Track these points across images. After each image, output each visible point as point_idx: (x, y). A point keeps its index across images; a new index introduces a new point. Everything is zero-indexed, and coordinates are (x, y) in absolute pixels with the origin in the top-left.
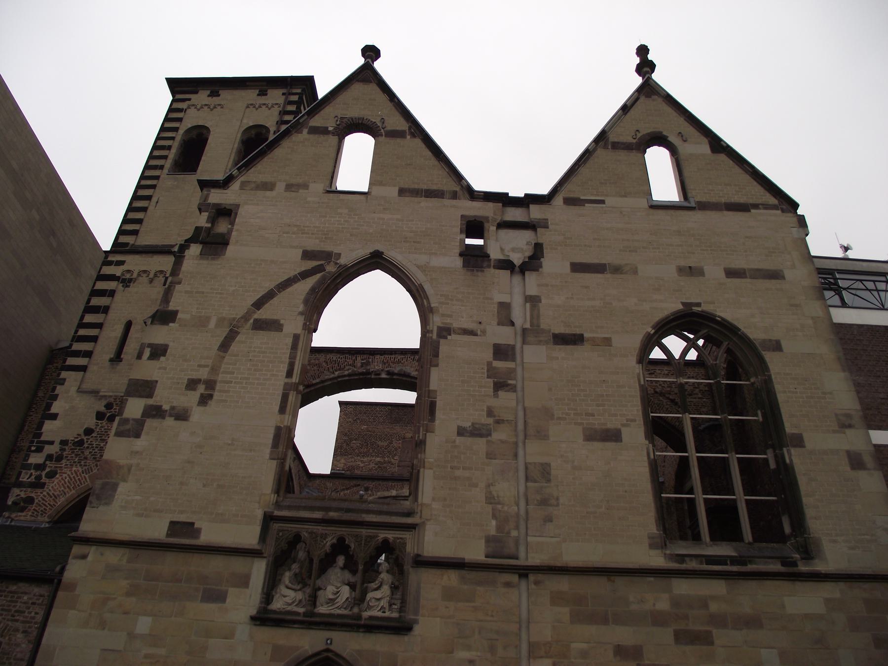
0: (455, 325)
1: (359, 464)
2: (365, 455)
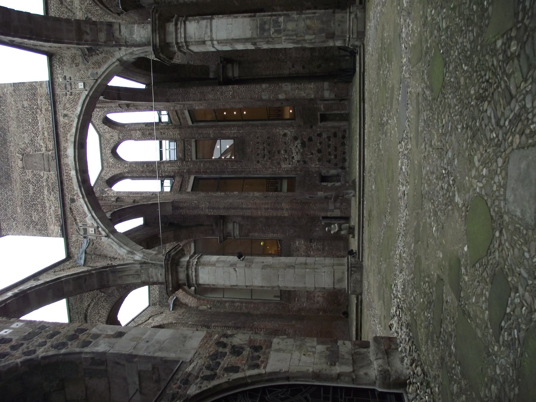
1: (53, 211)
2: (43, 206)
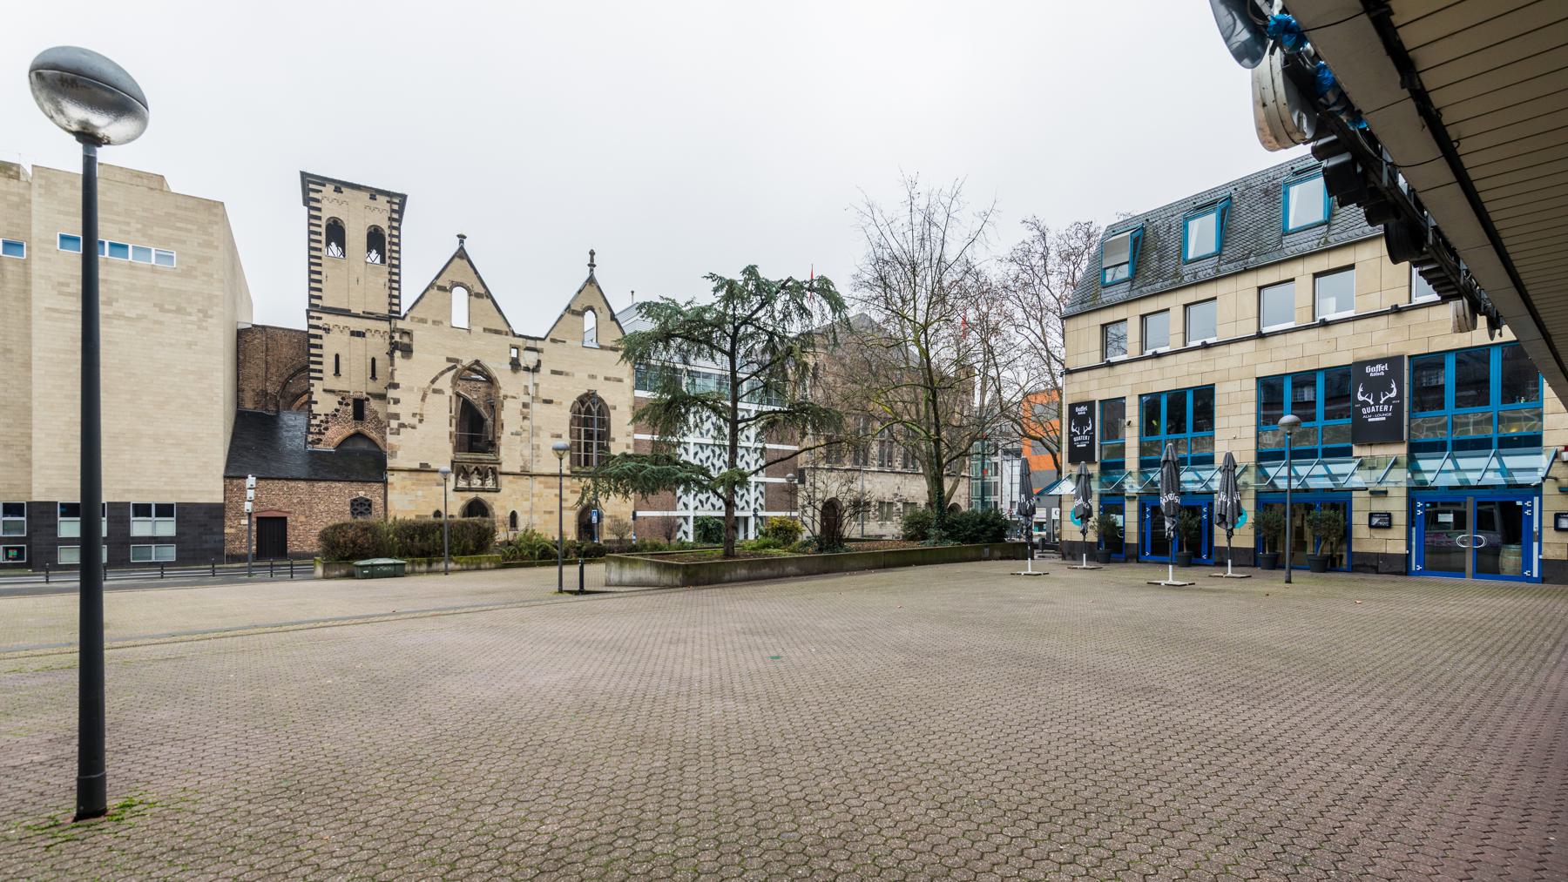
0: (509, 394)
